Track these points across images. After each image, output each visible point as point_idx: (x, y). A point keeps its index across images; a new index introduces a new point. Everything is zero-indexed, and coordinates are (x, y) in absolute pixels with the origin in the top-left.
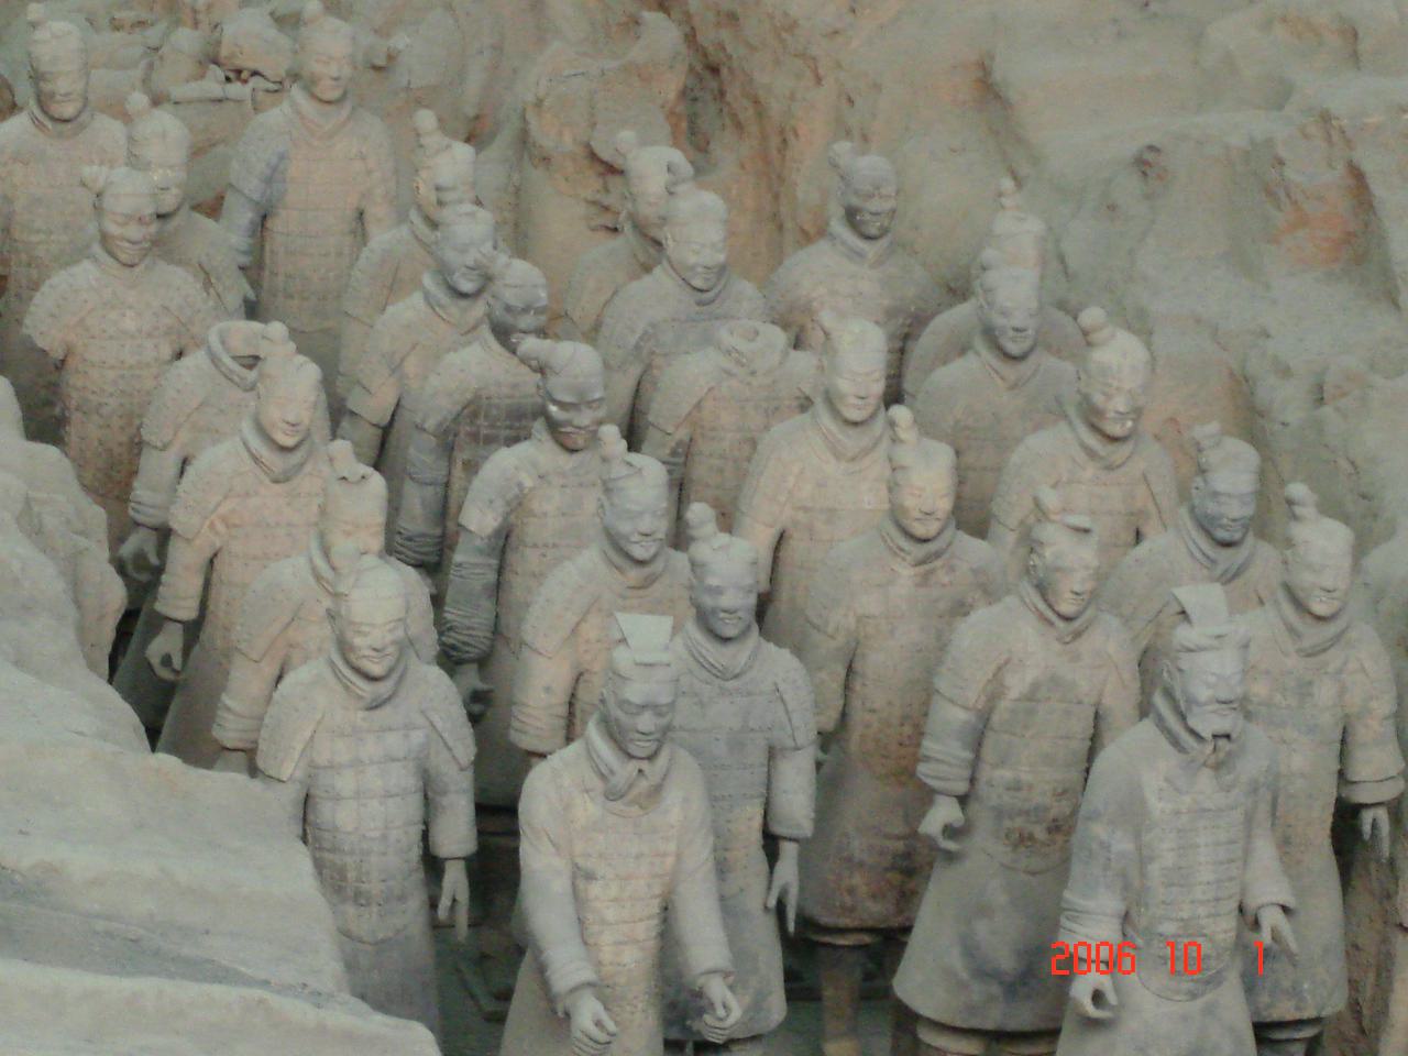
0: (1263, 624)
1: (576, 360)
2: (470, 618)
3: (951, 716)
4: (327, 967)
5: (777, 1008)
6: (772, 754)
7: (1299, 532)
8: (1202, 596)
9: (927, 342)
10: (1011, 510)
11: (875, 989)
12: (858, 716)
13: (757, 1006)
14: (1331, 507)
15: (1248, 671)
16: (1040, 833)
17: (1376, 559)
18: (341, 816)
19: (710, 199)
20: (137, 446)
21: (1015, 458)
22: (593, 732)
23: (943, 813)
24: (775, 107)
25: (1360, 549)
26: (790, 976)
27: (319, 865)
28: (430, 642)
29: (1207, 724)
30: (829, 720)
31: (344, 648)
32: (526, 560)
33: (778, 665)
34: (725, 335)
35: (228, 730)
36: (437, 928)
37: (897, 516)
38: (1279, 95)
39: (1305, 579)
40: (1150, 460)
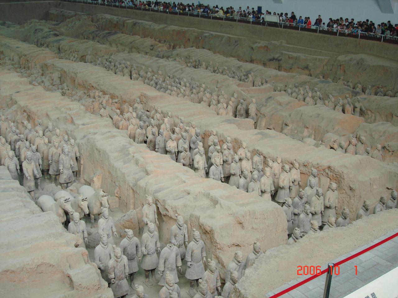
0: (69, 147)
1: (22, 136)
2: (17, 153)
3: (50, 155)
4: (11, 178)
5: (41, 175)
7: (71, 140)
8: (65, 145)
9: (45, 131)
10: (52, 142)
11: (48, 173)
12: (44, 156)
14: (73, 139)
15: (69, 150)
16: (57, 162)
17: (76, 141)
19: (30, 124)
21: (52, 138)
23: (50, 162)
24: (33, 118)
26: (42, 173)
27: (9, 171)
28: (15, 156)
29: (66, 153)
30: (42, 157)
31: (9, 157)
32: (21, 149)
33: (38, 153)
34: (32, 133)
35: (2, 163)
36: (18, 174)
37: (45, 143)
38: (66, 113)
39: (71, 143)
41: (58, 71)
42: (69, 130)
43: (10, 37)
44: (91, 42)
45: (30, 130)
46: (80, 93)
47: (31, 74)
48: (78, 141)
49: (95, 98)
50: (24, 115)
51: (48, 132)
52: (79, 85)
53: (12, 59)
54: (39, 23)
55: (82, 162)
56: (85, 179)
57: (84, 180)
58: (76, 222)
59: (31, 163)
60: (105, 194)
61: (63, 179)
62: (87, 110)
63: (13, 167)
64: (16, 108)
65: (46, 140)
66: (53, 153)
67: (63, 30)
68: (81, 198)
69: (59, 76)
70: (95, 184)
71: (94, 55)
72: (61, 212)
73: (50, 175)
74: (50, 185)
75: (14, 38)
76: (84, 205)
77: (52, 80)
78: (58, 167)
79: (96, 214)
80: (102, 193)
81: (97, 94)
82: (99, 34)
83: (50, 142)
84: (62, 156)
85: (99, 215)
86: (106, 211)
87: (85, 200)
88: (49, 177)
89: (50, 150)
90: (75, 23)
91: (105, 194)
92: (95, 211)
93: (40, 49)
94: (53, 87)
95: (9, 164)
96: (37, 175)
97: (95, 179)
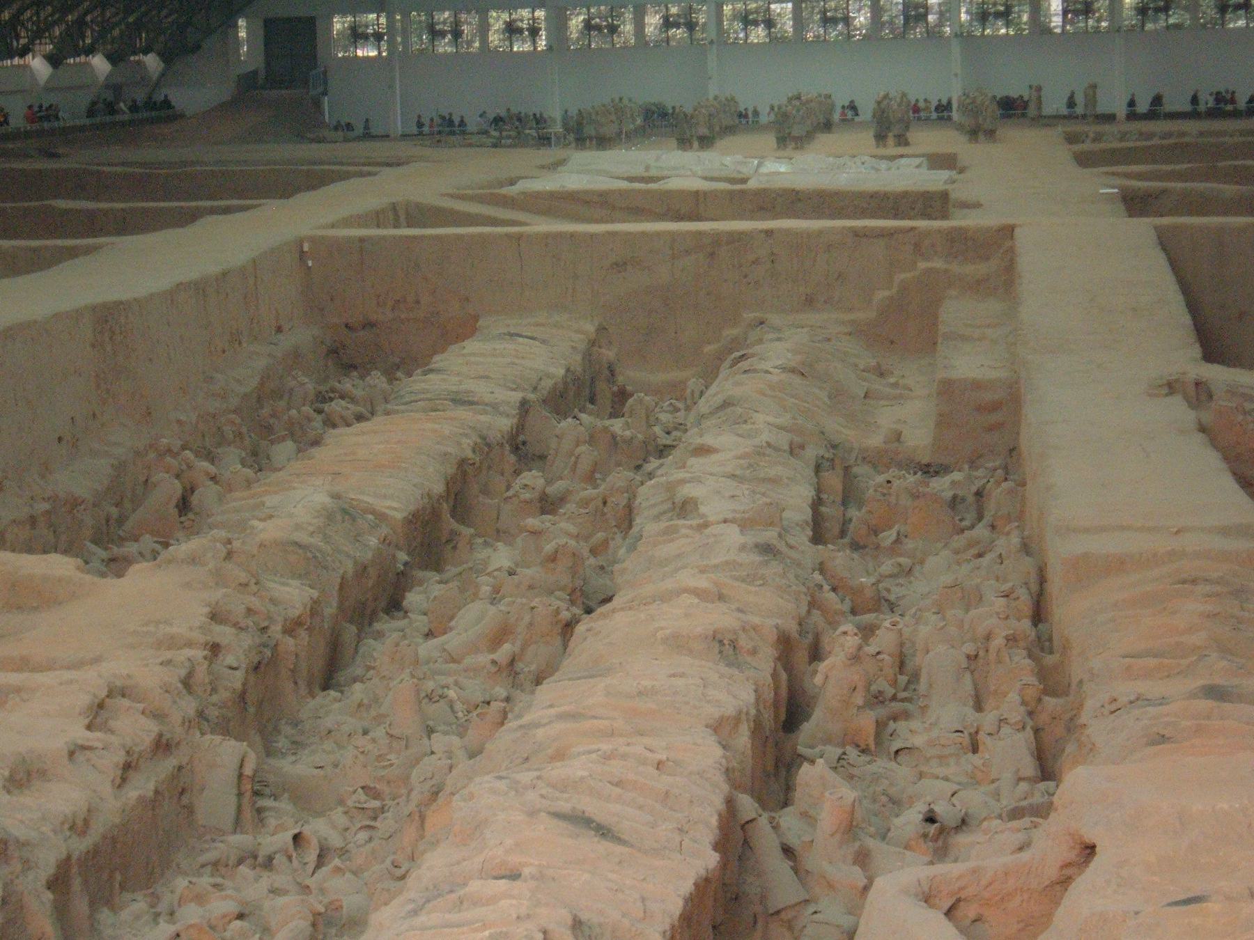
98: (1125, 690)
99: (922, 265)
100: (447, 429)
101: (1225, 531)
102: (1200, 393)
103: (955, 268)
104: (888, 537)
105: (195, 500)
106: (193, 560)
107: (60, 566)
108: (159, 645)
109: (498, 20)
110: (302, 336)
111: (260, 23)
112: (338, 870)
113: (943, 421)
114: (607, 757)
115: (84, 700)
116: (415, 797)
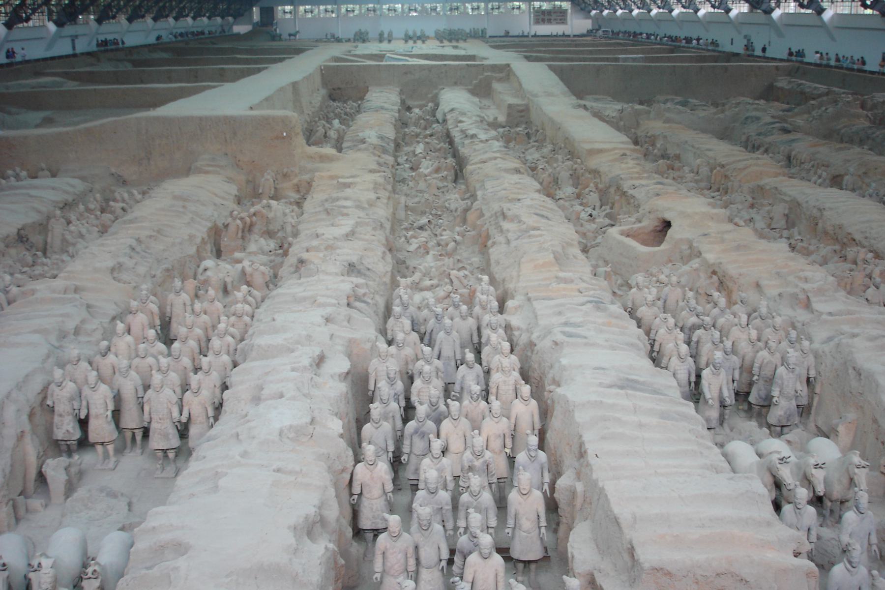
3: (756, 365)
5: (734, 402)
6: (734, 369)
7: (802, 342)
10: (764, 339)
12: (744, 365)
13: (731, 401)
18: (679, 376)
20: (650, 329)
22: (711, 366)
23: (755, 378)
25: (811, 344)
28: (689, 354)
32: (701, 344)
33: (735, 358)
34: (726, 316)
40: (782, 333)
41: (786, 202)
42: (798, 322)
43: (695, 130)
44: (857, 149)
45: (723, 311)
46: (826, 249)
47: (731, 204)
48: (816, 345)
49: (855, 263)
50: (712, 280)
51: (756, 318)
52: (826, 233)
53: (695, 170)
54: (755, 106)
55: (817, 390)
56: (820, 424)
57: (817, 427)
58: (799, 507)
59: (719, 375)
60: (863, 463)
61: (775, 415)
62: (839, 285)
63: (683, 376)
64: (697, 265)
65: (754, 334)
66: (763, 362)
67: (800, 121)
68: (812, 461)
69: (786, 212)
70: (839, 438)
71: (859, 176)
72: (769, 480)
73: (750, 404)
74: (749, 423)
75: (704, 131)
76: (818, 476)
77: (771, 218)
78: (770, 391)
79: (836, 501)
80: (856, 459)
81: (861, 256)
82: (873, 133)
83: (759, 340)
84: (781, 370)
85: (842, 502)
86: (864, 498)
87: (820, 467)
88: (746, 407)
89: (761, 353)
90: (826, 109)
91: (863, 463)
92: (837, 492)
93: (754, 155)
94: (772, 232)
95: (677, 368)
96: (727, 399)
97: (841, 429)
98: (637, 182)
99: (486, 74)
100: (387, 116)
101: (623, 143)
102: (585, 107)
103: (494, 75)
104: (512, 145)
105: (328, 135)
106: (366, 149)
107: (329, 150)
108: (371, 171)
109: (322, 8)
110: (323, 92)
111: (258, 9)
112: (445, 230)
113: (509, 115)
114: (532, 199)
115: (372, 186)
116: (459, 210)
